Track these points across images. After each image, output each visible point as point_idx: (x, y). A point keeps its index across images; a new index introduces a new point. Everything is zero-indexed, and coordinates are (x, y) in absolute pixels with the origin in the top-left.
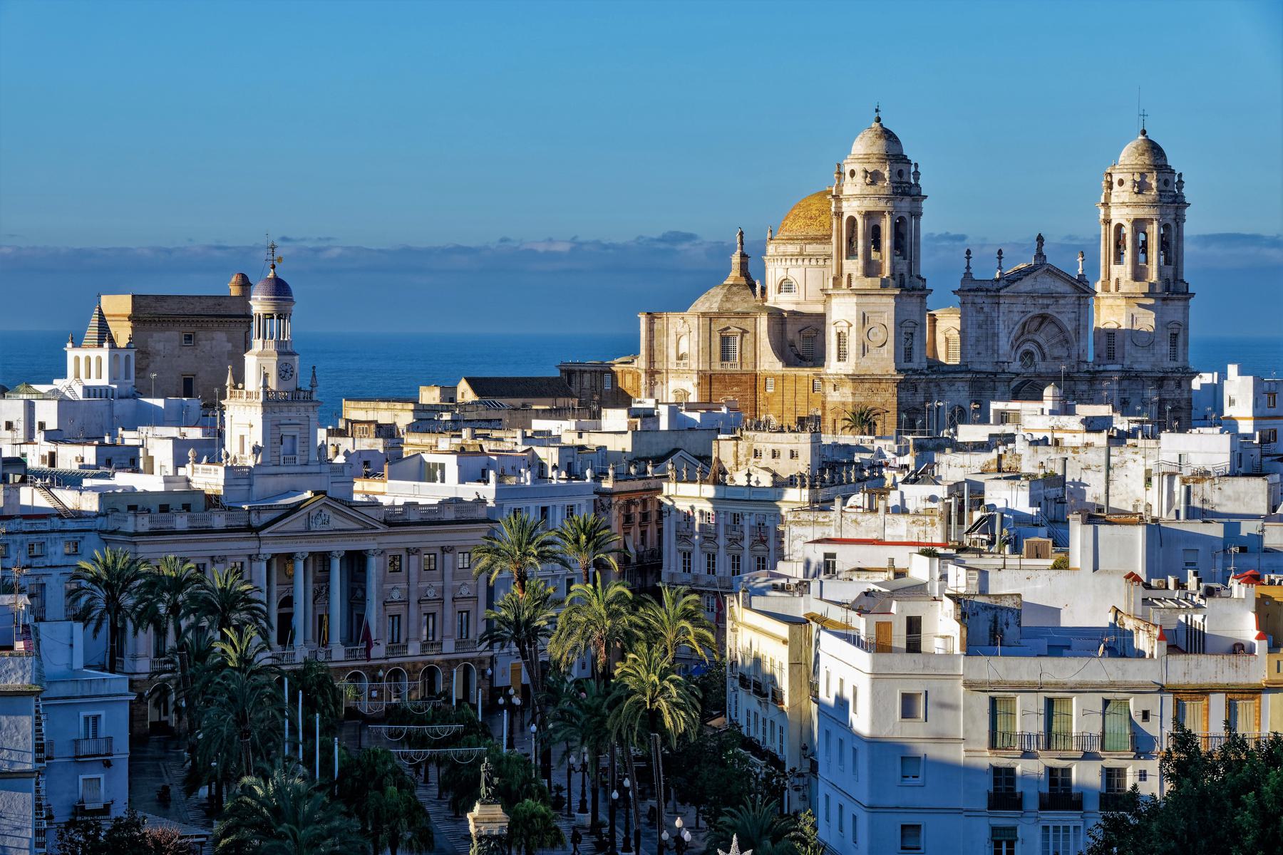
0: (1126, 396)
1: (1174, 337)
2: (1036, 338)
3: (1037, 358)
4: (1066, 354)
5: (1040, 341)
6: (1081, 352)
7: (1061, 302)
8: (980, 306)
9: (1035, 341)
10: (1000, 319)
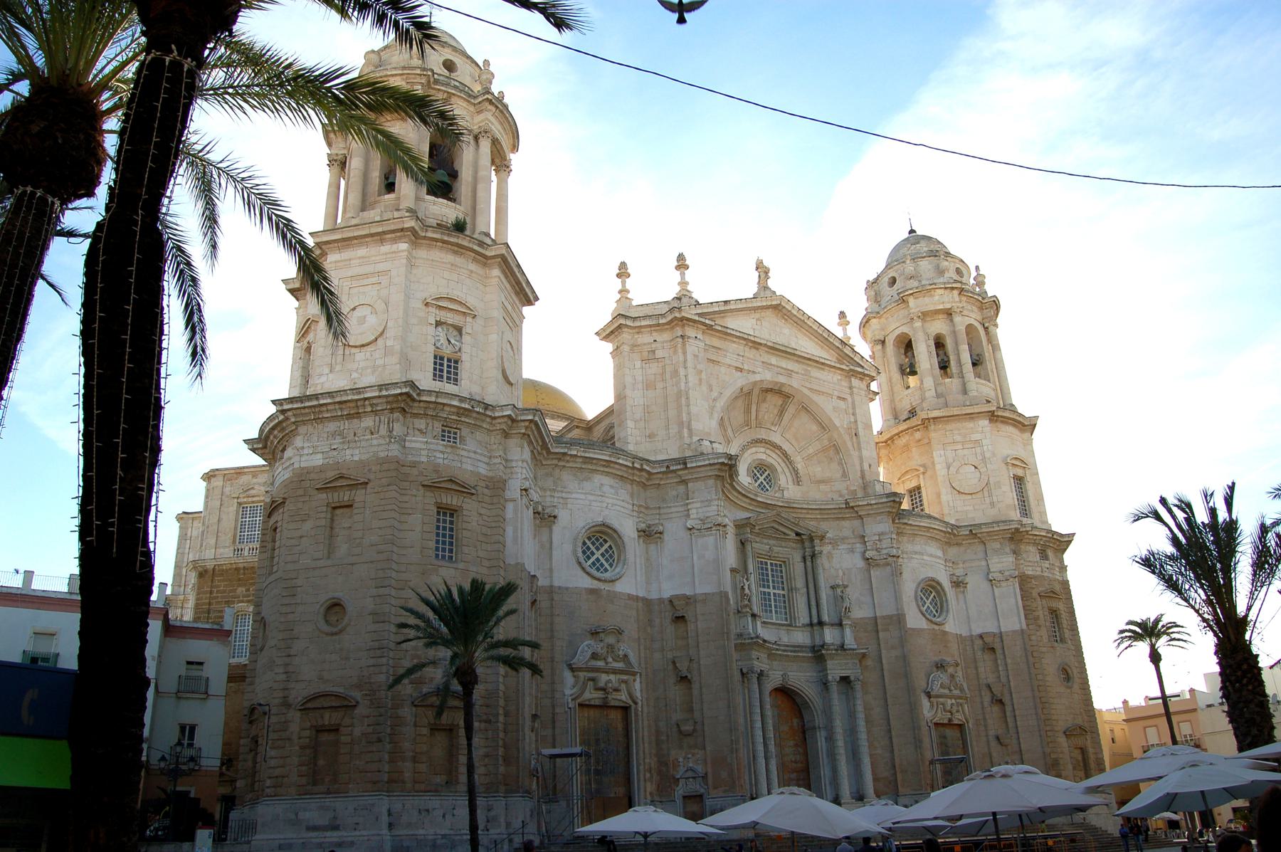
0: (959, 572)
1: (1019, 481)
2: (776, 438)
3: (784, 479)
4: (839, 475)
5: (786, 447)
6: (866, 467)
7: (815, 373)
8: (647, 348)
10: (689, 364)
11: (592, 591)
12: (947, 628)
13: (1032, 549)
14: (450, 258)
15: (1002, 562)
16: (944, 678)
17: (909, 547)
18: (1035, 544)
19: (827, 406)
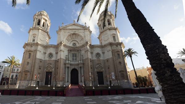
2: (76, 40)
5: (77, 40)
7: (79, 31)
9: (76, 41)
11: (49, 60)
12: (100, 59)
13: (115, 46)
14: (35, 30)
15: (109, 48)
16: (98, 65)
17: (95, 49)
18: (115, 45)
19: (81, 34)
